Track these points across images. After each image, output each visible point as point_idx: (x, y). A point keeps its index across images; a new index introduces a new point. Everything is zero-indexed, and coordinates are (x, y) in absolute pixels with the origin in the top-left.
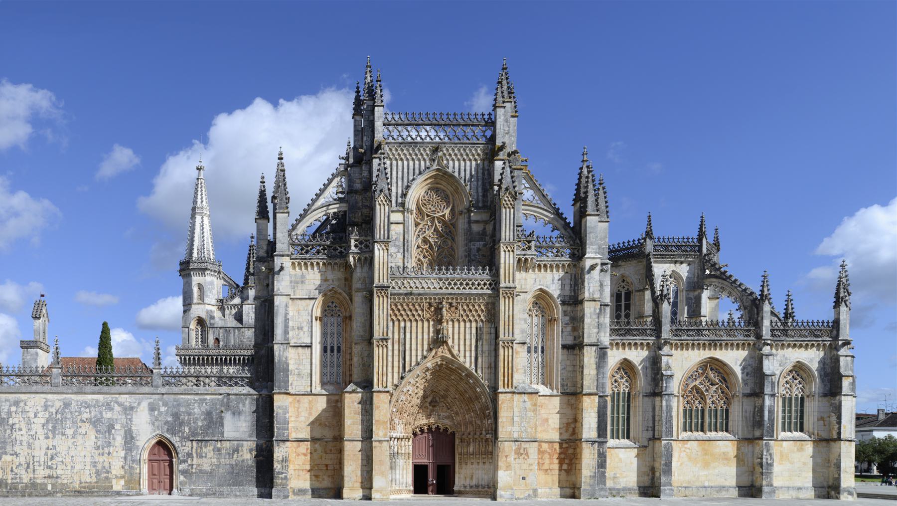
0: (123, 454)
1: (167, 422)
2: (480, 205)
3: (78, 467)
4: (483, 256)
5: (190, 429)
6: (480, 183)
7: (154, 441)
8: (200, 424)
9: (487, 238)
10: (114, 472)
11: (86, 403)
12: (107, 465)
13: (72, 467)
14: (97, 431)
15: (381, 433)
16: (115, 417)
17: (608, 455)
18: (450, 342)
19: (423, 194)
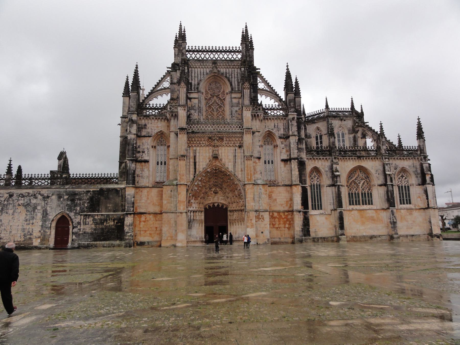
0: (40, 223)
1: (67, 205)
2: (237, 89)
3: (13, 232)
4: (239, 114)
5: (80, 208)
6: (236, 79)
7: (59, 216)
8: (86, 205)
9: (241, 106)
10: (34, 234)
11: (22, 194)
12: (30, 230)
13: (10, 232)
14: (27, 211)
15: (182, 208)
16: (38, 202)
17: (310, 218)
18: (220, 158)
19: (208, 85)
